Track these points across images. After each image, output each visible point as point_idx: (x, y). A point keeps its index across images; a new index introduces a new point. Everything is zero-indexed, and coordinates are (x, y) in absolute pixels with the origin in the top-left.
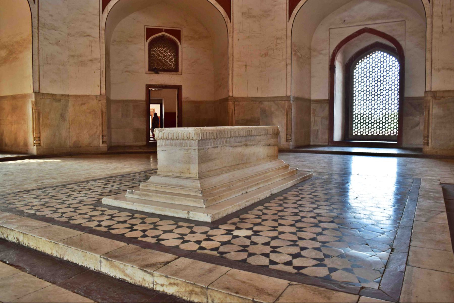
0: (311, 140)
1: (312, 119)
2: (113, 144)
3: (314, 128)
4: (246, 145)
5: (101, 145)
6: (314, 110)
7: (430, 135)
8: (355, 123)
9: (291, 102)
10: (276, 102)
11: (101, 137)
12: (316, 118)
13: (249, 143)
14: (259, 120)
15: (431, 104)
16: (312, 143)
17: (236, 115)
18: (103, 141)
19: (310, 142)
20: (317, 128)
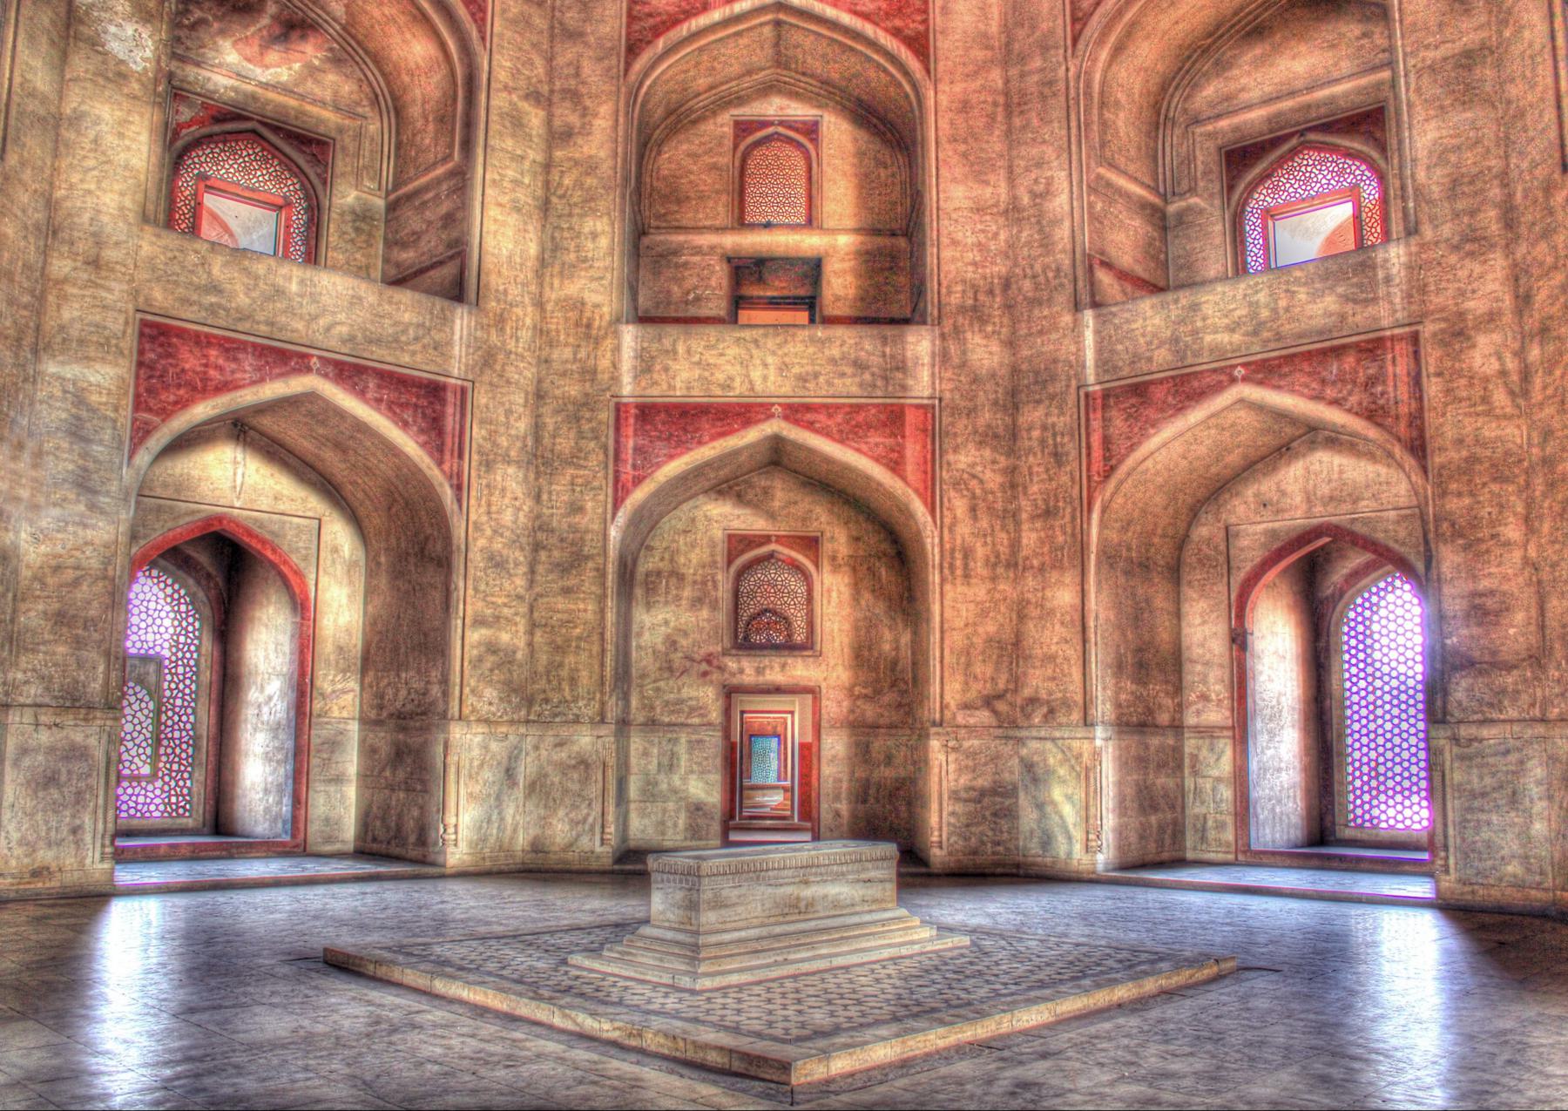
0: (1189, 844)
1: (1189, 783)
2: (632, 844)
3: (1197, 810)
4: (806, 883)
5: (598, 849)
6: (1194, 757)
7: (1451, 841)
8: (1353, 791)
9: (1098, 743)
10: (1060, 743)
11: (598, 829)
12: (1200, 781)
13: (812, 879)
14: (1015, 788)
15: (1447, 756)
16: (1190, 855)
17: (951, 777)
18: (602, 840)
19: (1184, 849)
20: (1203, 810)
